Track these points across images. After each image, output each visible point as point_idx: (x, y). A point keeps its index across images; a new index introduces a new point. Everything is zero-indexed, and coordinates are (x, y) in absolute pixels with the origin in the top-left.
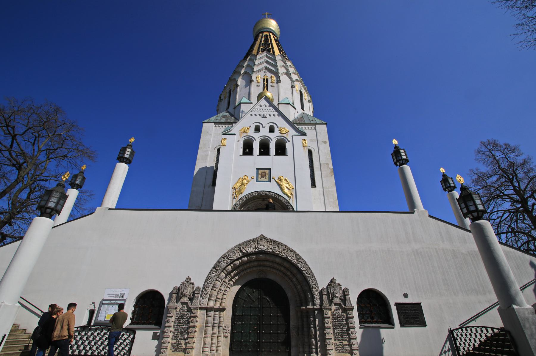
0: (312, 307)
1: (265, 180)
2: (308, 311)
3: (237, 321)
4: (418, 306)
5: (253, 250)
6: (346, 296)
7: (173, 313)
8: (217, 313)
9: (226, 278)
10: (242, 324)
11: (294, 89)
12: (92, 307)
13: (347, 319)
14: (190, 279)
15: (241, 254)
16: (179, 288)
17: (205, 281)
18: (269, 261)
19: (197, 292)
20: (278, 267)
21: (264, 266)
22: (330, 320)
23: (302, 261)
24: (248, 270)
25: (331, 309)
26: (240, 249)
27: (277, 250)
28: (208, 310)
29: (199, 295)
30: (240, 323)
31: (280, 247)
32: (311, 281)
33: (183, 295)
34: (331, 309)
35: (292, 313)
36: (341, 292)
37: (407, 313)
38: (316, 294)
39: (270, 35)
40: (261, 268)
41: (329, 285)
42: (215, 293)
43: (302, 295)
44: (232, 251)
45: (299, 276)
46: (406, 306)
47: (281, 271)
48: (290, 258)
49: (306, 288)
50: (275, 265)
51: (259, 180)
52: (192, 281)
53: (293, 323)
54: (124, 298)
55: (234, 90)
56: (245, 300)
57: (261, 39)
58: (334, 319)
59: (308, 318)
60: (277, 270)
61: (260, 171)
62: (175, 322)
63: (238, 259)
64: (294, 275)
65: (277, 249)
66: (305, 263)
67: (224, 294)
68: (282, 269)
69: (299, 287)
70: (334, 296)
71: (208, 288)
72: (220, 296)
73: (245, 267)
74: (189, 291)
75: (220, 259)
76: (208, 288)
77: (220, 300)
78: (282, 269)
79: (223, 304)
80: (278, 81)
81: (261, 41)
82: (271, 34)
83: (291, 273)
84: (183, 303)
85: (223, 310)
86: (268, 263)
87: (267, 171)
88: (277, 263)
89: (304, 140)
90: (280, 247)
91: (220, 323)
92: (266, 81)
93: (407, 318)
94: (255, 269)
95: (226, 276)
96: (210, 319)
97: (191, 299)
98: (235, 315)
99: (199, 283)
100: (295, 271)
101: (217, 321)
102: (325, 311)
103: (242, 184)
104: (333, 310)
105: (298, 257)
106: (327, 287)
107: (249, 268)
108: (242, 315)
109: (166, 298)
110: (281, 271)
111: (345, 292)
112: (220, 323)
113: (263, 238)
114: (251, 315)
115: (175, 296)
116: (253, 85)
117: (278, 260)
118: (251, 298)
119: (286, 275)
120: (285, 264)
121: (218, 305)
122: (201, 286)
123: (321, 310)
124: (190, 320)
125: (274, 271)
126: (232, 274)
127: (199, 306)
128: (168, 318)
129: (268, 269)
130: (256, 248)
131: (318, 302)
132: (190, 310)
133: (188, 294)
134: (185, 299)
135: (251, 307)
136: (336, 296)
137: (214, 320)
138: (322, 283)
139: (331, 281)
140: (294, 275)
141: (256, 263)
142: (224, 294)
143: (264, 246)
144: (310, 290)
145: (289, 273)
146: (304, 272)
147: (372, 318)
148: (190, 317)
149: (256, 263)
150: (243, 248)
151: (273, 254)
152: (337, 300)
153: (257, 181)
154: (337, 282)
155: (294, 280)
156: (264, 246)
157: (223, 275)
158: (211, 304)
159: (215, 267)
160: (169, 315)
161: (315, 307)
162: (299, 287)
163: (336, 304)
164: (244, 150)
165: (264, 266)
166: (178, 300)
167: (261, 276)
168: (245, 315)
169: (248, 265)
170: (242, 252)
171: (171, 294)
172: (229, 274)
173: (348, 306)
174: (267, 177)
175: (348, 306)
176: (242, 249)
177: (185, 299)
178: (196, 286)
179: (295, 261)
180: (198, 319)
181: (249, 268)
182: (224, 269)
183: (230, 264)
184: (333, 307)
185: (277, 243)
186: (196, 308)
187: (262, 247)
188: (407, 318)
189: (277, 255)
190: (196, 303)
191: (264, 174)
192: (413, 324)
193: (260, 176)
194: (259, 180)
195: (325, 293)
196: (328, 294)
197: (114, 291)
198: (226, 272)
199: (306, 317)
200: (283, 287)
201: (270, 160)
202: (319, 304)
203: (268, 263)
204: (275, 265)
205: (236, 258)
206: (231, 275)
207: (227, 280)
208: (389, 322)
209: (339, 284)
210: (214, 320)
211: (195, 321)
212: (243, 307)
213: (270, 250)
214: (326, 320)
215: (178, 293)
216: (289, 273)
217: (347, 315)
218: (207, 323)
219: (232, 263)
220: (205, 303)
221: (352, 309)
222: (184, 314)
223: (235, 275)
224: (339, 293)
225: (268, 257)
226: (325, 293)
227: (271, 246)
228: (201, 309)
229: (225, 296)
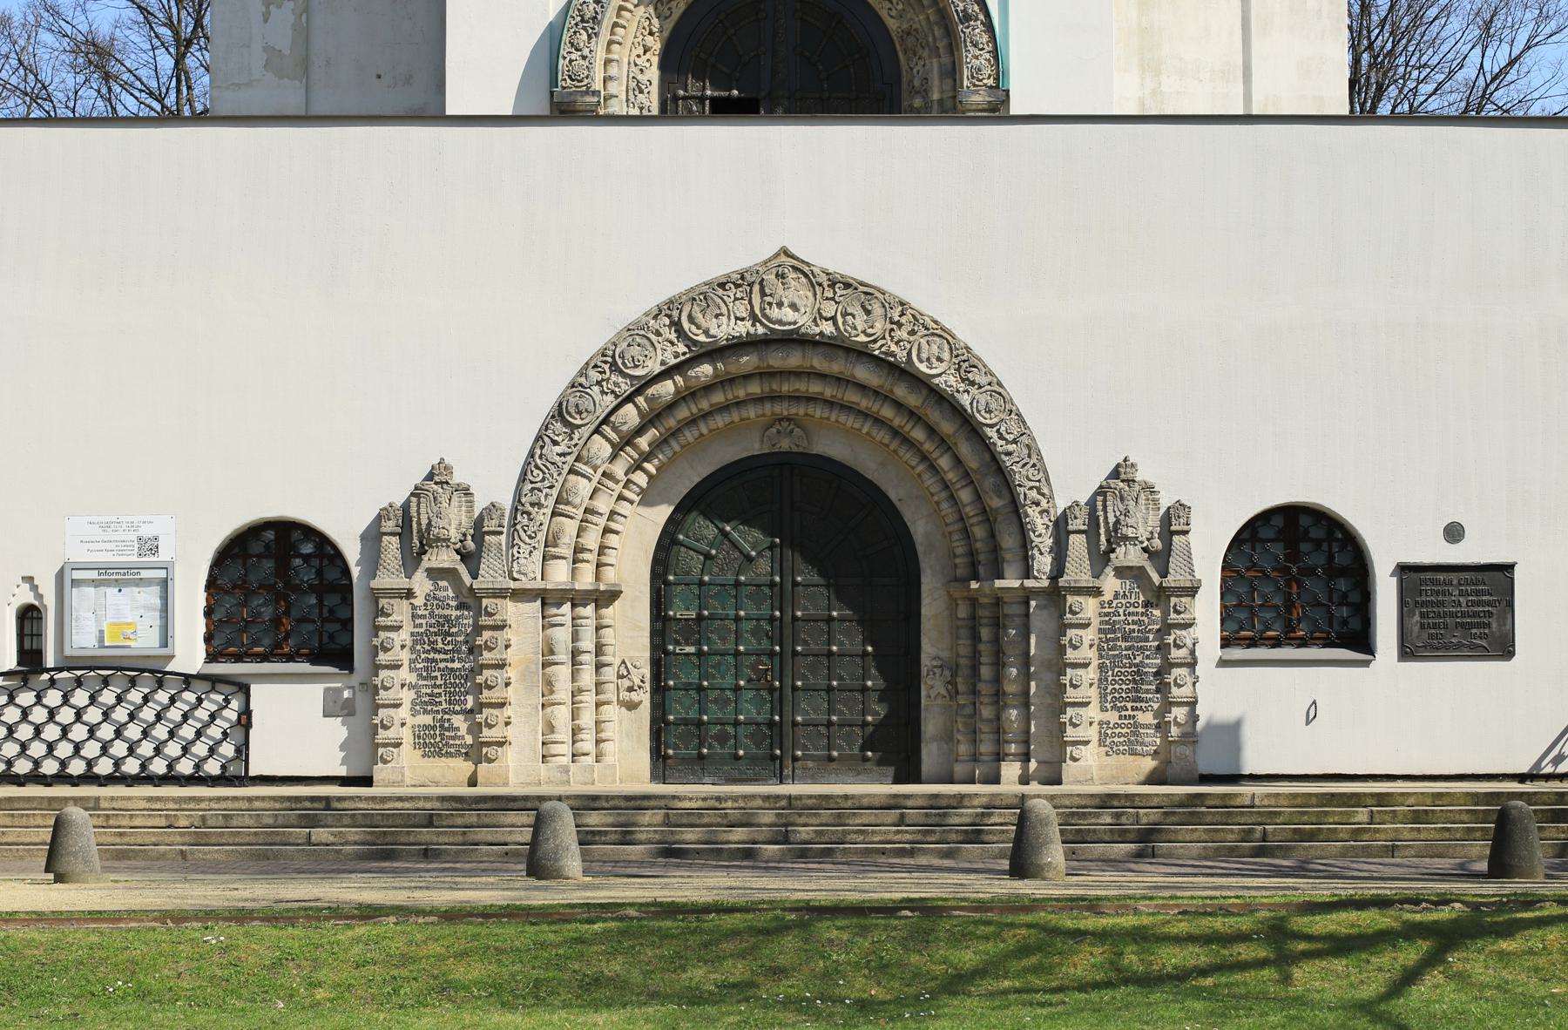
0: (1016, 584)
2: (998, 600)
3: (677, 643)
5: (743, 328)
6: (1176, 538)
7: (400, 612)
8: (589, 610)
9: (613, 458)
10: (700, 654)
13: (1166, 628)
14: (448, 469)
15: (681, 348)
16: (406, 507)
17: (523, 478)
18: (823, 376)
19: (489, 525)
20: (865, 403)
21: (796, 398)
22: (1089, 635)
23: (983, 380)
24: (720, 421)
25: (1096, 592)
26: (676, 325)
27: (859, 328)
28: (548, 599)
29: (503, 538)
30: (692, 649)
31: (877, 310)
32: (1021, 475)
33: (428, 541)
34: (1096, 592)
35: (932, 606)
36: (1154, 521)
37: (1441, 604)
38: (1041, 529)
40: (781, 409)
41: (1101, 491)
42: (570, 527)
43: (979, 532)
44: (636, 331)
45: (964, 449)
46: (1441, 577)
47: (879, 421)
48: (923, 367)
49: (996, 502)
50: (852, 396)
52: (458, 478)
53: (932, 647)
54: (164, 556)
56: (708, 556)
58: (1109, 628)
59: (998, 624)
60: (865, 415)
62: (413, 650)
63: (667, 373)
64: (944, 444)
65: (860, 321)
66: (997, 390)
67: (607, 531)
68: (887, 412)
69: (965, 495)
70: (1117, 538)
71: (539, 505)
72: (592, 540)
73: (705, 405)
74: (454, 521)
75: (583, 373)
76: (539, 505)
77: (592, 557)
78: (887, 412)
79: (610, 575)
83: (932, 431)
84: (434, 574)
85: (612, 596)
86: (815, 388)
88: (862, 388)
90: (877, 310)
91: (599, 649)
93: (1435, 626)
94: (751, 412)
95: (617, 449)
96: (562, 636)
97: (470, 559)
98: (667, 619)
99: (494, 486)
100: (947, 427)
101: (587, 643)
102: (1070, 599)
104: (1108, 596)
105: (966, 363)
106: (1092, 503)
107: (724, 408)
108: (700, 618)
109: (352, 552)
110: (879, 421)
111: (1172, 525)
112: (599, 649)
113: (788, 264)
114: (737, 619)
115: (392, 545)
117: (863, 373)
118: (735, 545)
119: (907, 441)
120: (901, 392)
121: (586, 581)
122: (506, 501)
123: (1055, 595)
124: (479, 641)
125: (849, 421)
126: (643, 442)
127: (513, 585)
128: (383, 635)
129: (818, 412)
130: (755, 319)
131: (1043, 563)
132: (470, 600)
133: (454, 535)
134: (444, 558)
135: (737, 584)
136: (1126, 538)
137: (575, 637)
139: (1115, 474)
140: (944, 444)
141: (755, 388)
142: (607, 531)
143: (797, 310)
144: (1015, 508)
145: (918, 434)
146: (992, 433)
147: (1289, 628)
148: (478, 629)
149: (755, 388)
150: (691, 319)
151: (837, 346)
152: (1129, 555)
154: (1139, 476)
155: (944, 462)
156: (794, 307)
157: (601, 448)
158: (560, 574)
159: (559, 413)
160: (382, 621)
161: (1029, 583)
162: (965, 495)
163: (1121, 572)
165: (796, 398)
166: (412, 560)
167: (785, 445)
168: (712, 617)
169: (718, 397)
170: (690, 342)
171: (372, 538)
172: (628, 440)
173: (1175, 578)
175: (1172, 580)
176: (686, 325)
177: (444, 558)
178: (480, 505)
179: (948, 381)
180: (507, 634)
181: (724, 408)
182: (605, 421)
183: (629, 399)
184: (1110, 584)
185: (865, 293)
186: (500, 594)
187: (788, 314)
188: (1435, 626)
189: (860, 353)
190: (491, 574)
192: (1459, 646)
195: (1078, 523)
196: (1091, 532)
197: (105, 526)
198: (613, 436)
199: (992, 629)
200: (893, 496)
202: (1048, 569)
203: (815, 388)
204: (852, 396)
205: (658, 369)
206: (635, 447)
207: (619, 469)
208: (1360, 640)
209: (1149, 489)
210: (575, 637)
211: (501, 643)
212: (701, 583)
213: (827, 328)
214: (1071, 633)
215: (408, 530)
216: (918, 434)
217: (1166, 614)
218: (552, 652)
219: (639, 391)
220: (530, 570)
221: (1192, 591)
222: (447, 619)
223: (656, 446)
224: (1143, 524)
225: (818, 362)
226: (1078, 523)
227: (829, 309)
228: (519, 595)
229: (612, 540)
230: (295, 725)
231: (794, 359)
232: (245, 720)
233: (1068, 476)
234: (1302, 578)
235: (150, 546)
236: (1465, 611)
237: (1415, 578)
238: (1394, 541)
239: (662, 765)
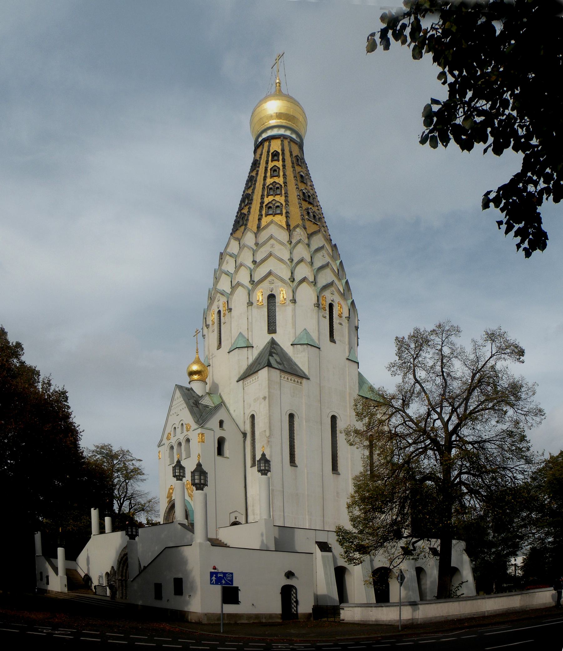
55: (225, 315)
82: (286, 142)
92: (271, 297)
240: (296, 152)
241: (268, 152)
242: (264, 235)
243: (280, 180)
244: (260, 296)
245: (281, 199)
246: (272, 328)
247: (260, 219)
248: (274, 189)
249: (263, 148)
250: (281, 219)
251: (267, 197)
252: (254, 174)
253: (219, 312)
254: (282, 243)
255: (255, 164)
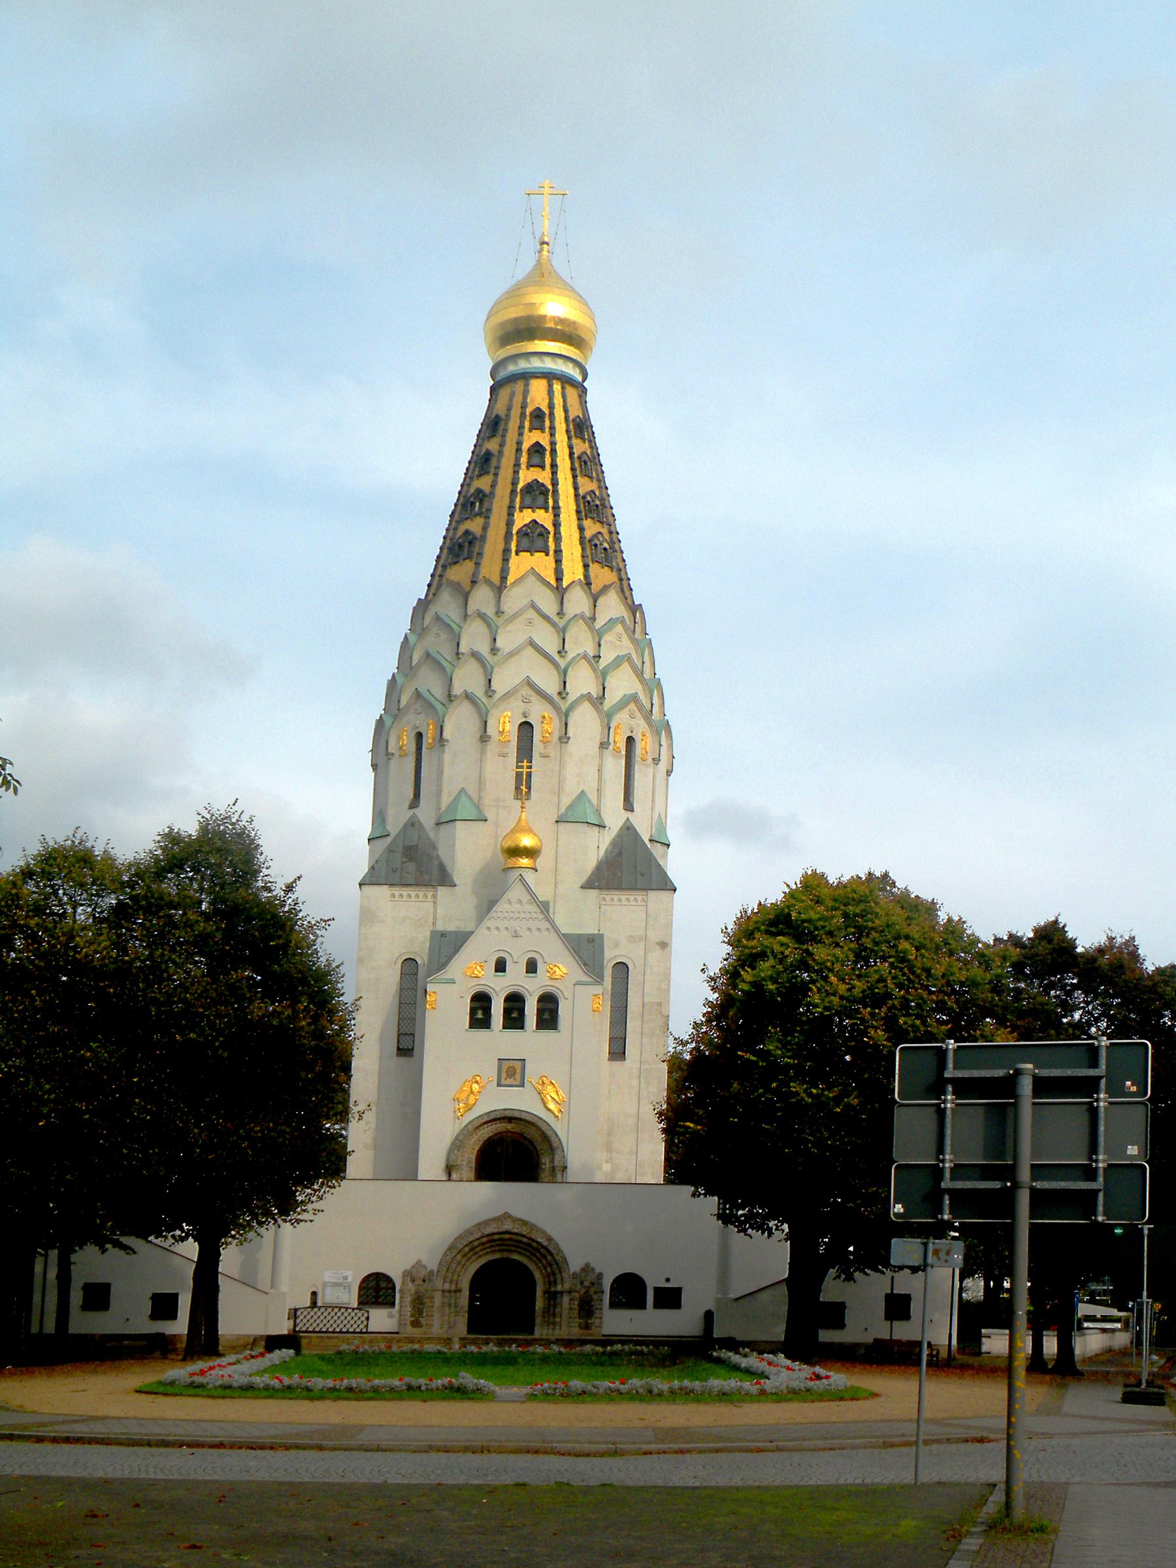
1: (514, 1083)
4: (678, 1291)
11: (607, 754)
12: (314, 1289)
39: (551, 406)
45: (549, 1258)
51: (503, 1082)
57: (519, 450)
61: (506, 1065)
80: (564, 738)
81: (517, 465)
82: (557, 387)
85: (460, 1291)
87: (519, 1064)
89: (595, 995)
92: (526, 727)
103: (472, 1092)
111: (600, 1276)
116: (492, 747)
121: (453, 1288)
138: (575, 1265)
153: (499, 1085)
164: (473, 1011)
174: (518, 1077)
191: (511, 1072)
193: (504, 1075)
194: (503, 1082)
201: (528, 1041)
209: (593, 1269)
230: (381, 1320)
231: (507, 1236)
232: (368, 1319)
233: (575, 1265)
234: (629, 1290)
235: (345, 1278)
236: (669, 1298)
237: (657, 1290)
238: (653, 1281)
239: (470, 1331)
240: (575, 411)
241: (524, 406)
242: (513, 600)
243: (544, 477)
244: (505, 723)
245: (544, 518)
246: (523, 785)
247: (506, 560)
248: (537, 494)
249: (513, 394)
250: (543, 563)
251: (521, 511)
252: (492, 445)
253: (419, 736)
254: (546, 618)
255: (493, 425)
